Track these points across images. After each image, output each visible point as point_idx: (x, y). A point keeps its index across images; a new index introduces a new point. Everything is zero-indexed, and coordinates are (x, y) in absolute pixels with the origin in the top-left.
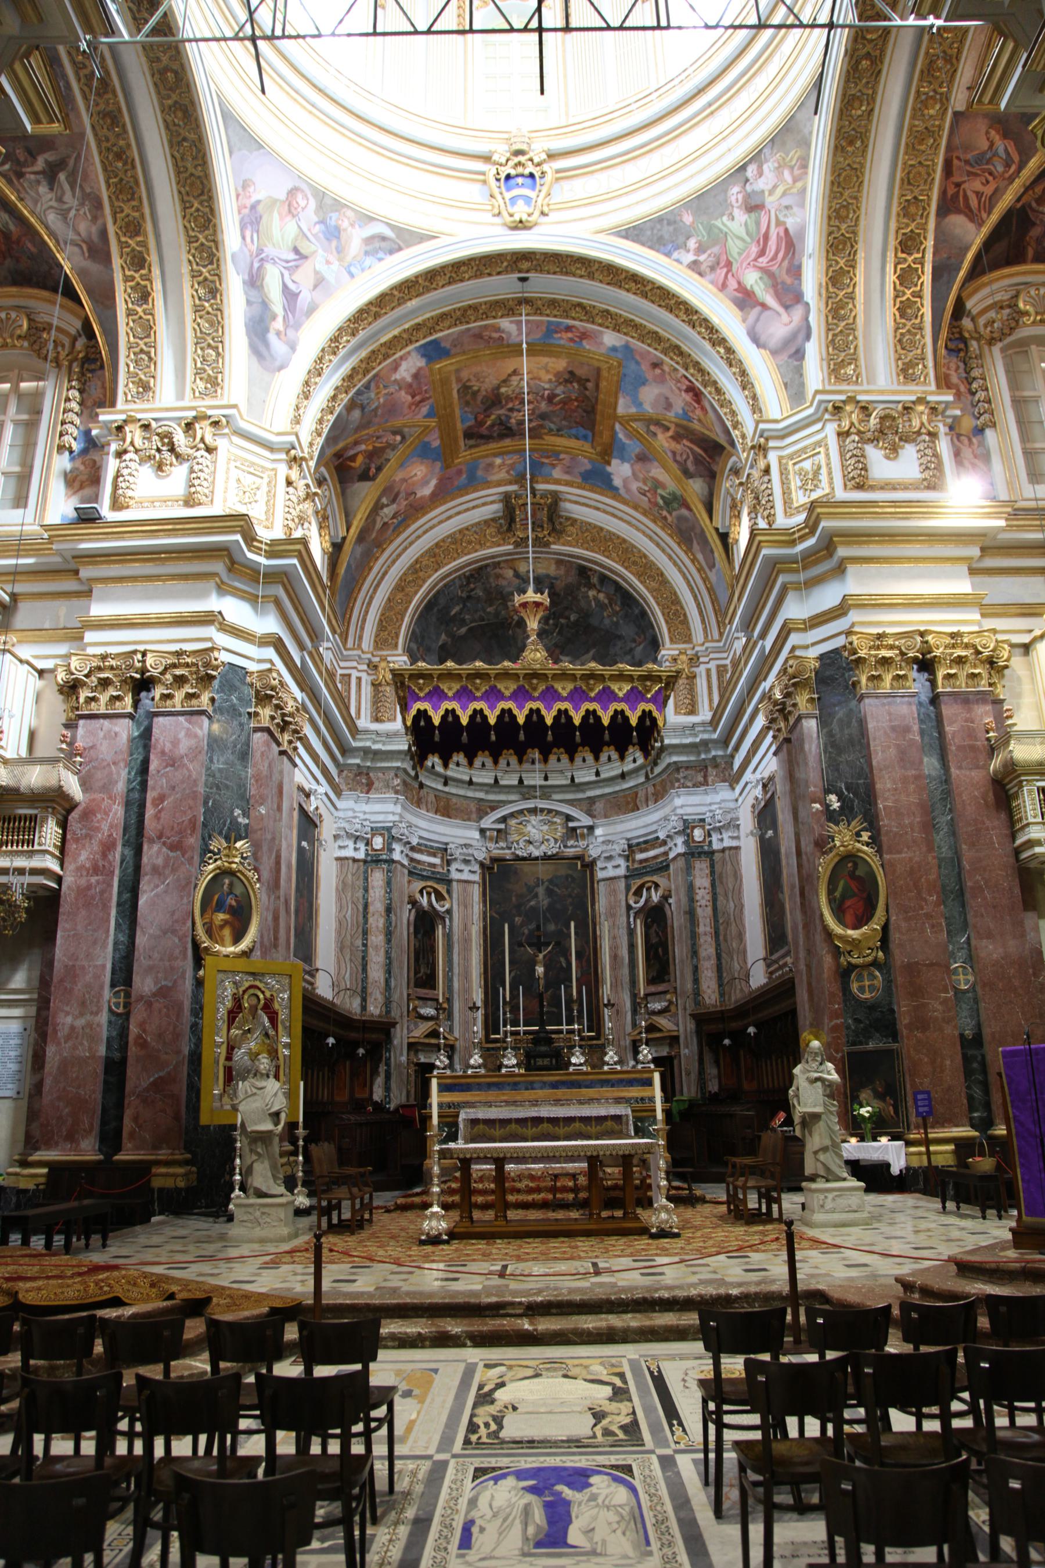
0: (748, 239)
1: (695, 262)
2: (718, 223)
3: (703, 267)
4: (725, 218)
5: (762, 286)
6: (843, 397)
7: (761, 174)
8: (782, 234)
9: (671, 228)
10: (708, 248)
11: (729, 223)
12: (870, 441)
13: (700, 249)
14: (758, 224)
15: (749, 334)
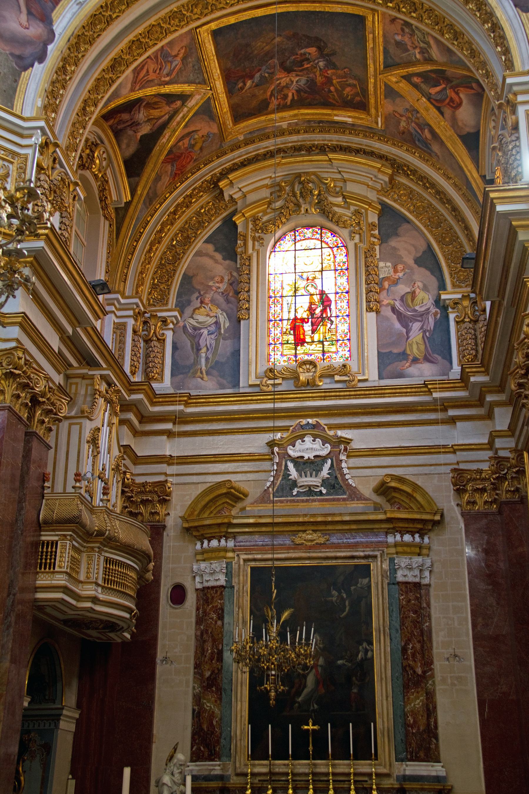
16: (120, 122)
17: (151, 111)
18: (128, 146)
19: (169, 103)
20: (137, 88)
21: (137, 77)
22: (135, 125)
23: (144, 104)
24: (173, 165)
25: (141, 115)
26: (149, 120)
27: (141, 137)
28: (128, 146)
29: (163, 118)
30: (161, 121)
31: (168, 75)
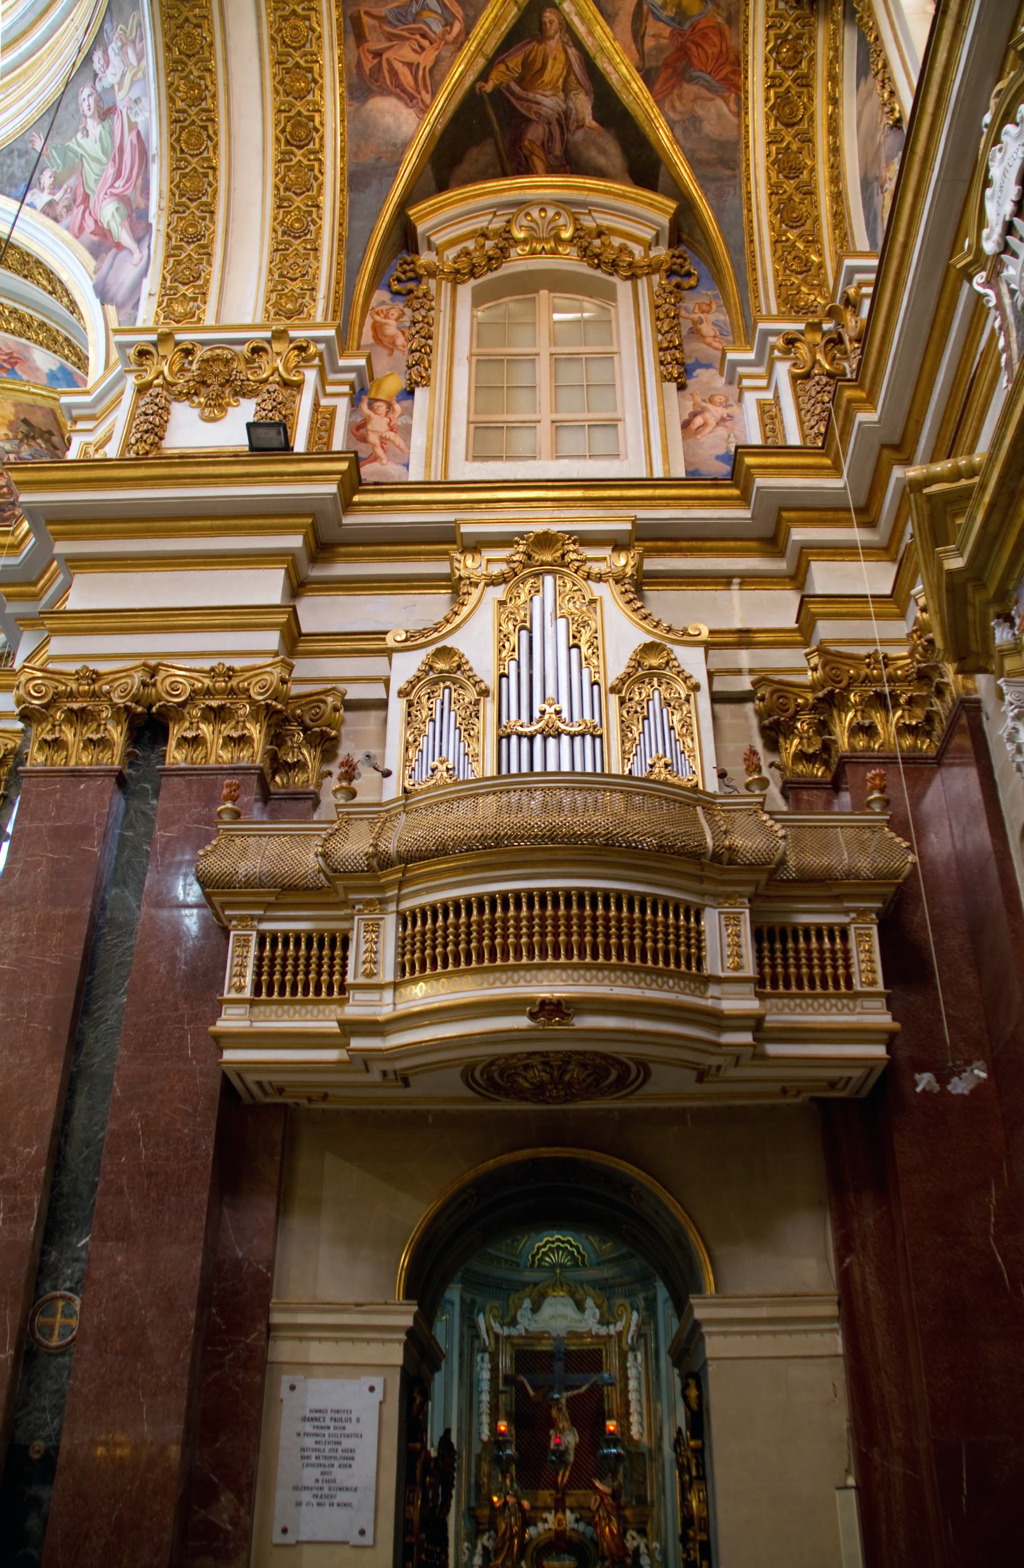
0: (104, 159)
1: (51, 204)
2: (72, 144)
3: (60, 209)
4: (79, 135)
5: (119, 220)
6: (154, 337)
7: (107, 63)
8: (135, 141)
9: (23, 161)
10: (64, 182)
11: (82, 141)
12: (179, 397)
13: (56, 186)
14: (112, 134)
15: (95, 287)
16: (546, 147)
17: (547, 77)
18: (603, 152)
19: (541, 34)
20: (427, 97)
21: (404, 91)
22: (564, 120)
23: (517, 89)
24: (691, 80)
25: (549, 102)
26: (566, 90)
27: (594, 118)
28: (603, 152)
29: (573, 59)
30: (576, 67)
31: (448, 24)
